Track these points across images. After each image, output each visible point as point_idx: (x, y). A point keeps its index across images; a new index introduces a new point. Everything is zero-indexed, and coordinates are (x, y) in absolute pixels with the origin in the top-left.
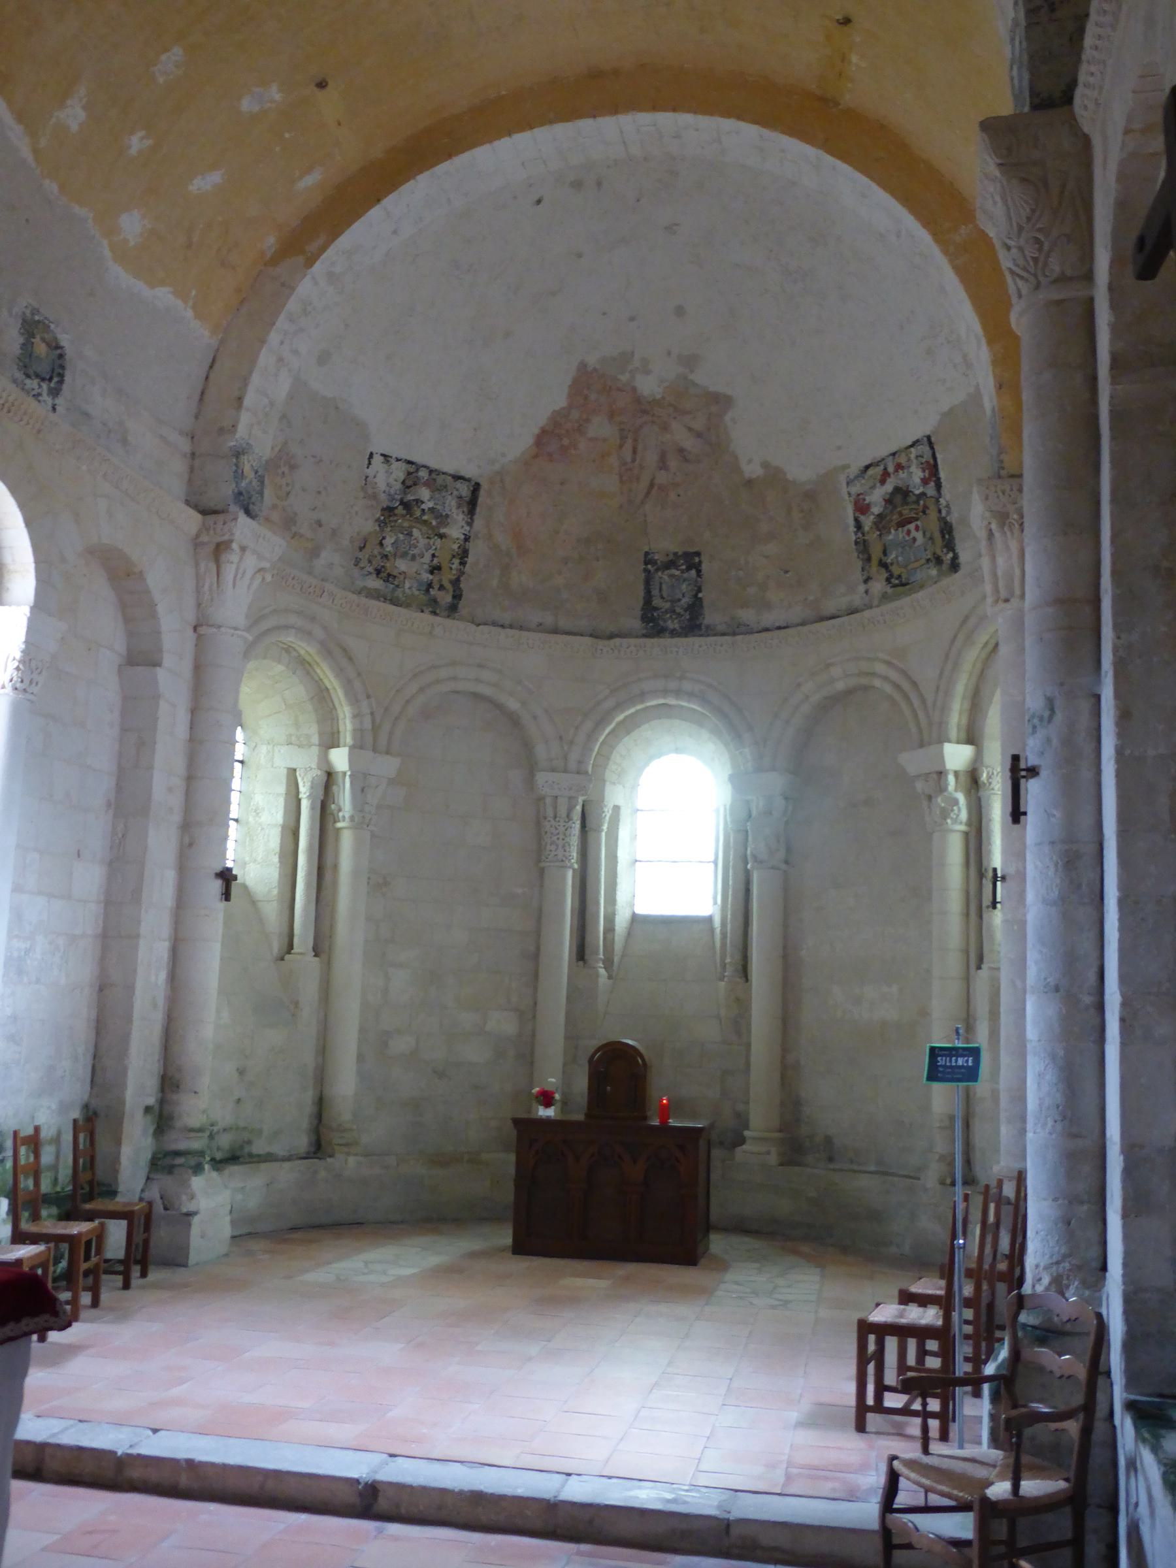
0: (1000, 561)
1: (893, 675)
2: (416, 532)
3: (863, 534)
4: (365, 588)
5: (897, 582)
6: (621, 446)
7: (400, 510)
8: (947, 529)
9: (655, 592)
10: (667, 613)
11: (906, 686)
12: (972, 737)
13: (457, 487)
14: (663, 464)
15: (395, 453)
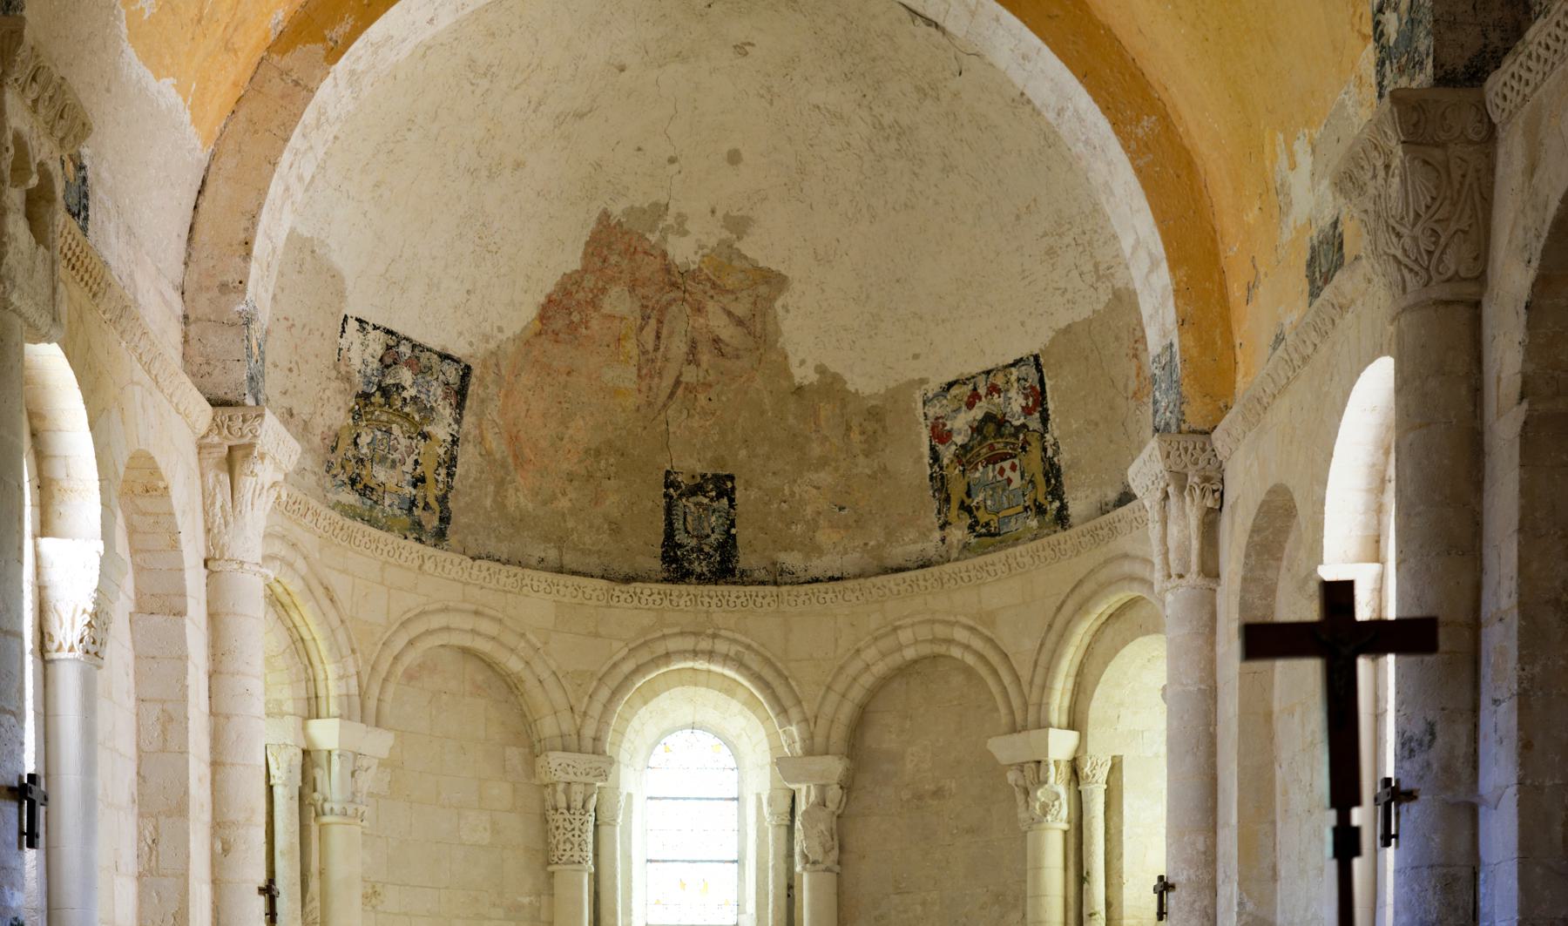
0: (1173, 530)
1: (977, 644)
2: (396, 429)
3: (941, 468)
4: (339, 502)
5: (983, 530)
6: (642, 329)
7: (378, 398)
8: (1053, 472)
9: (678, 525)
10: (693, 552)
11: (994, 659)
13: (443, 369)
14: (692, 357)
15: (372, 319)
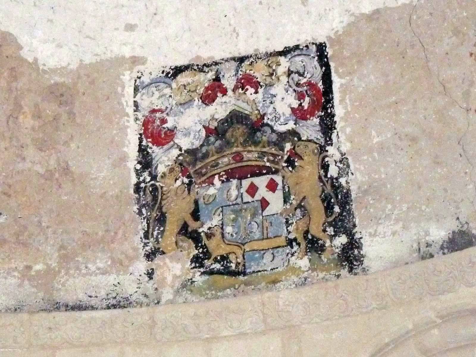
3: (154, 177)
5: (217, 266)
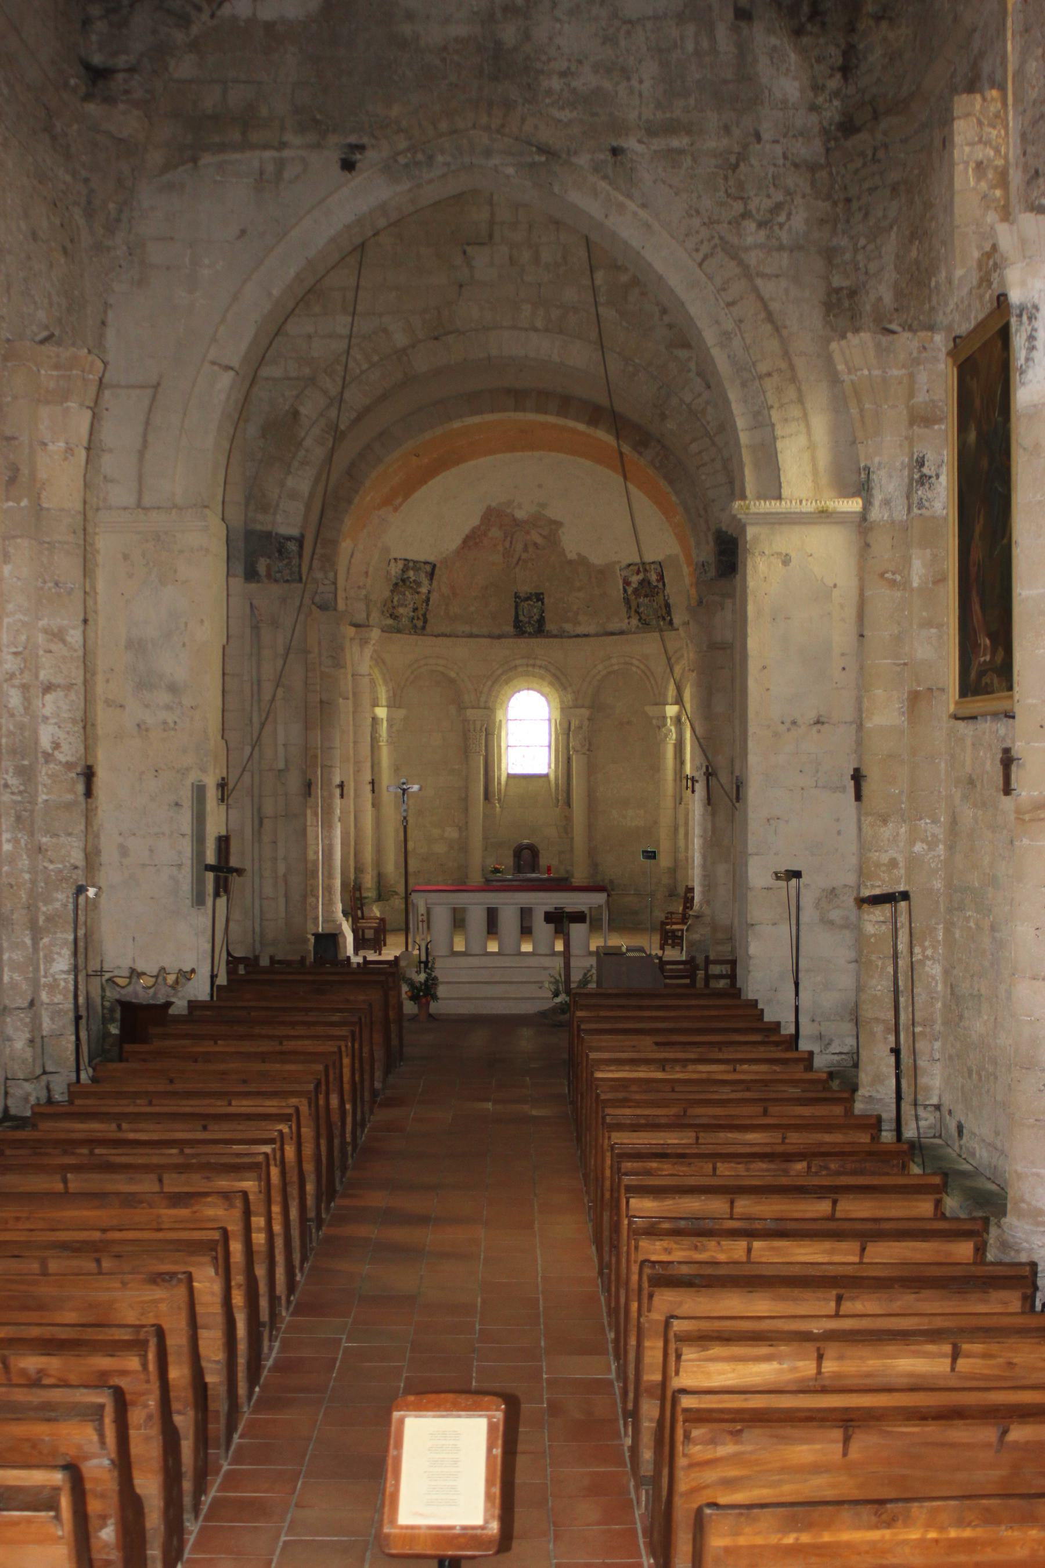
1: (642, 666)
11: (649, 674)
12: (679, 701)
